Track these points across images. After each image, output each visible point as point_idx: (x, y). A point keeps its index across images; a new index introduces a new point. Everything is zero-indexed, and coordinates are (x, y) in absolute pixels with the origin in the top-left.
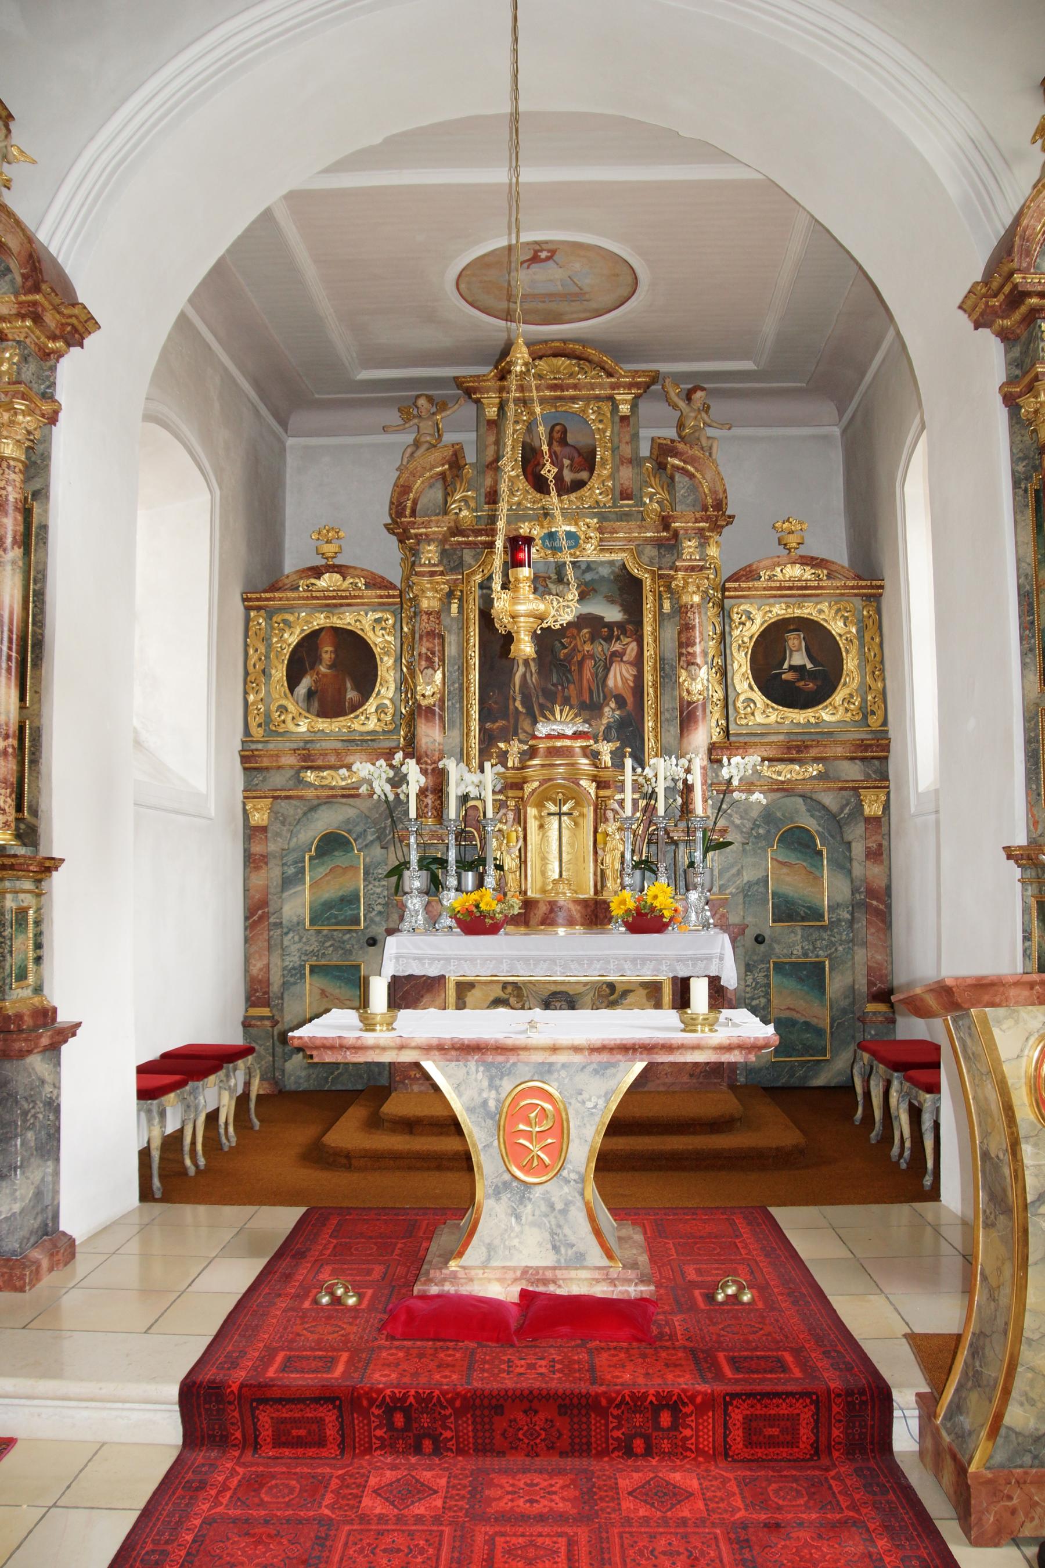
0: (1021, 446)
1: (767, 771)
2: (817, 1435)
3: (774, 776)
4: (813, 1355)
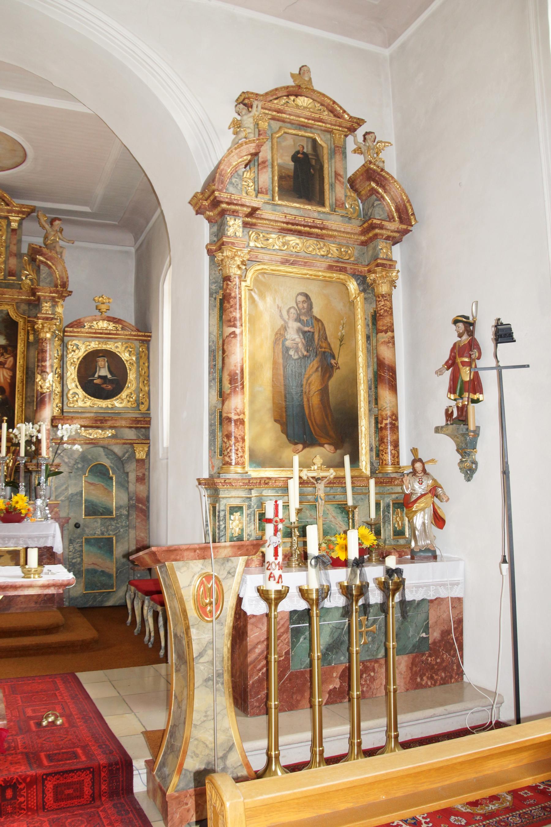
0: (214, 276)
1: (84, 432)
2: (93, 790)
3: (88, 436)
4: (93, 748)
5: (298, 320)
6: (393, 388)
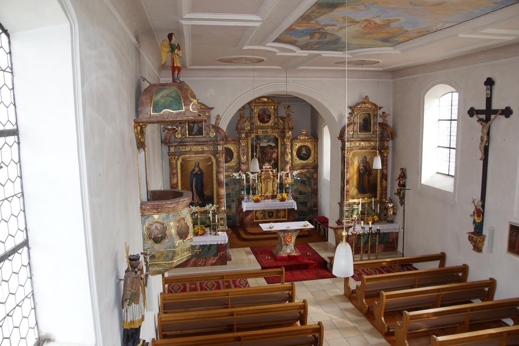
5: (363, 163)
6: (386, 180)
